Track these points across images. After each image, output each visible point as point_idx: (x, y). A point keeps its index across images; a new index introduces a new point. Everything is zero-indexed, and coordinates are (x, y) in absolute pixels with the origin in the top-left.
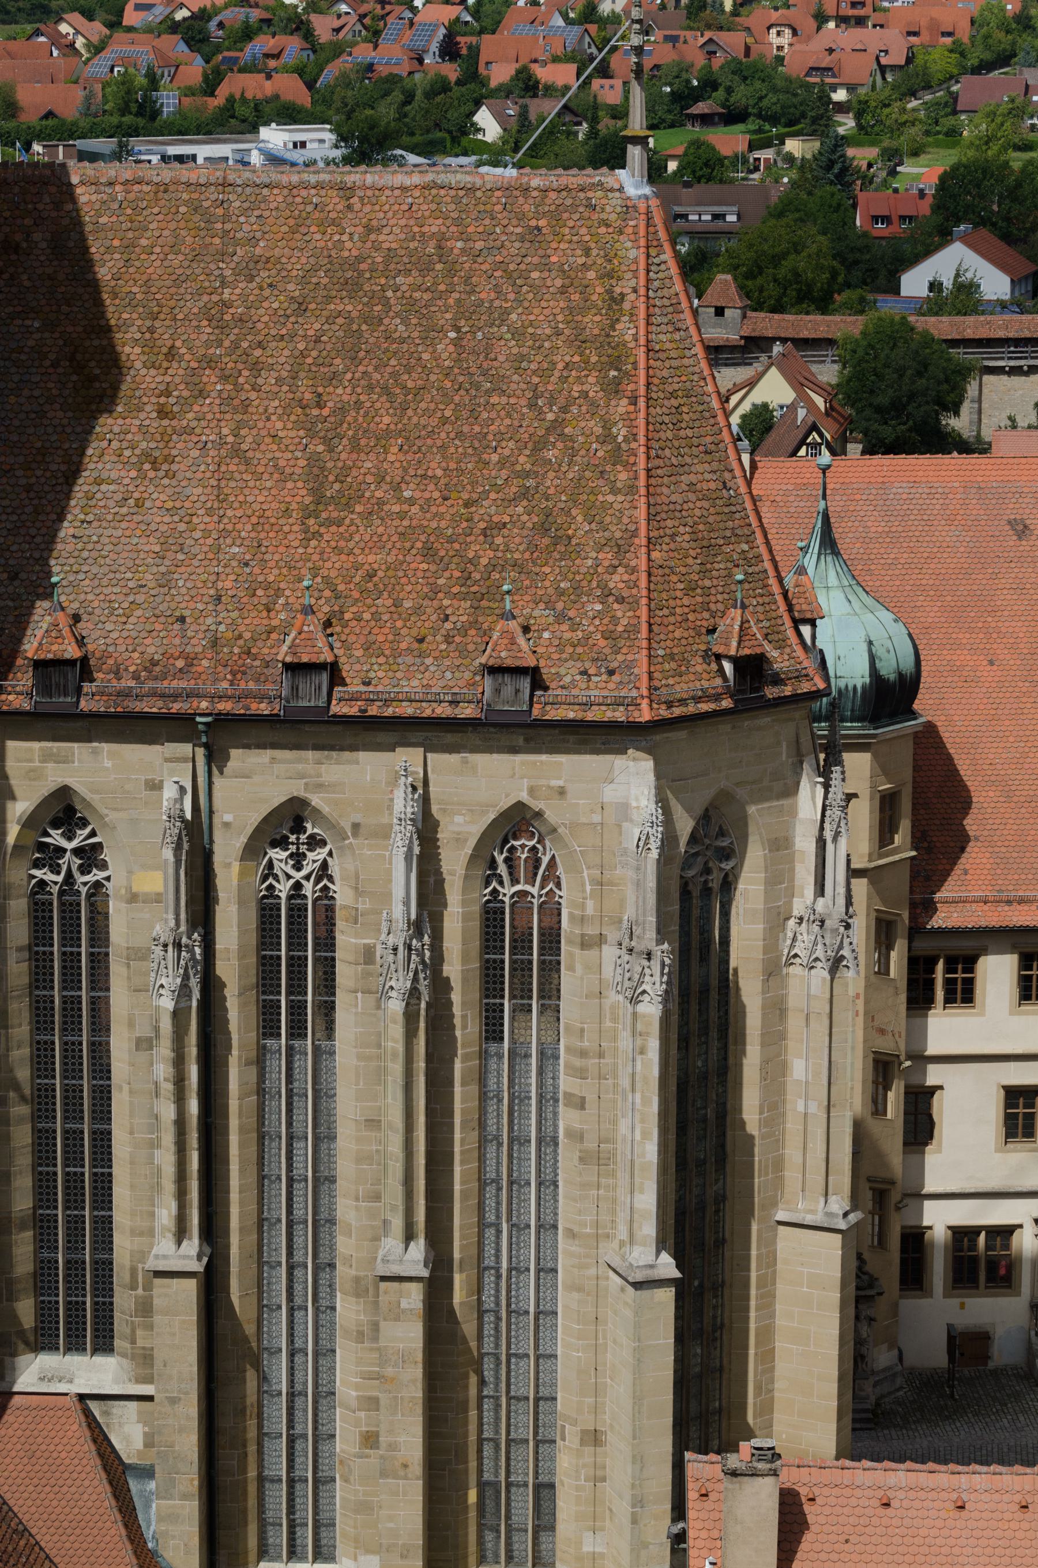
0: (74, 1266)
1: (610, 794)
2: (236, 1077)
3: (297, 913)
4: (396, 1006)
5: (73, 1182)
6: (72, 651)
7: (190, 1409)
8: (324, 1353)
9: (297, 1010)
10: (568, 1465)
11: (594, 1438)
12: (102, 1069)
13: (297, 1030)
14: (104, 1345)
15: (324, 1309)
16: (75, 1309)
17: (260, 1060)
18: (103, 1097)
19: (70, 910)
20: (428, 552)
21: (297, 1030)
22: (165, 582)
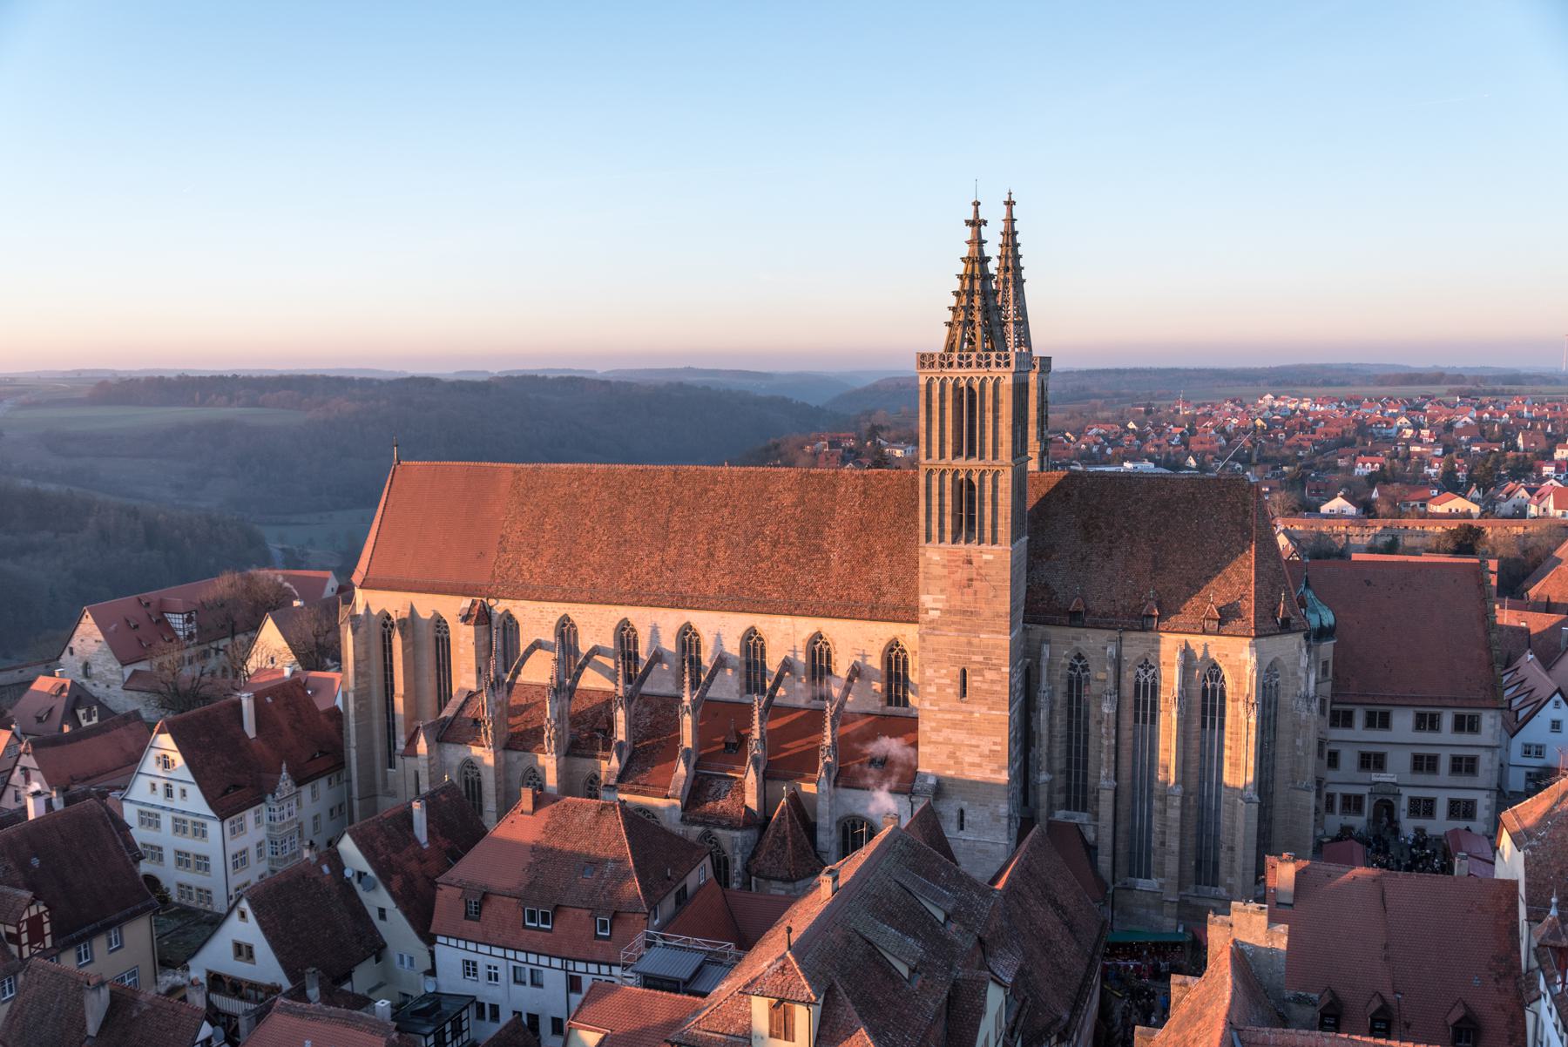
0: (1077, 786)
1: (1242, 657)
2: (1126, 734)
3: (1145, 687)
4: (1175, 715)
5: (1077, 761)
6: (1082, 609)
7: (1109, 830)
8: (1150, 816)
9: (1145, 715)
10: (1224, 855)
11: (1232, 849)
12: (1087, 730)
13: (1144, 721)
14: (1084, 810)
15: (1150, 804)
16: (1076, 798)
17: (1134, 729)
18: (1086, 737)
19: (1079, 683)
20: (1188, 584)
21: (1144, 721)
22: (1109, 590)
